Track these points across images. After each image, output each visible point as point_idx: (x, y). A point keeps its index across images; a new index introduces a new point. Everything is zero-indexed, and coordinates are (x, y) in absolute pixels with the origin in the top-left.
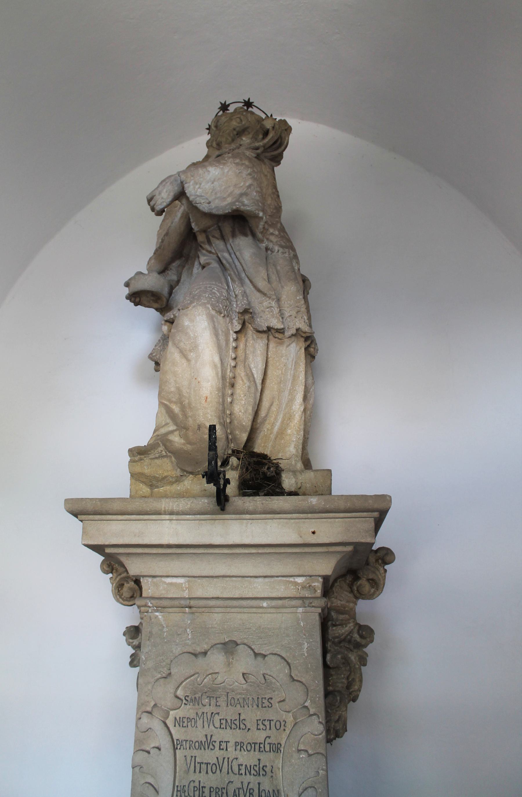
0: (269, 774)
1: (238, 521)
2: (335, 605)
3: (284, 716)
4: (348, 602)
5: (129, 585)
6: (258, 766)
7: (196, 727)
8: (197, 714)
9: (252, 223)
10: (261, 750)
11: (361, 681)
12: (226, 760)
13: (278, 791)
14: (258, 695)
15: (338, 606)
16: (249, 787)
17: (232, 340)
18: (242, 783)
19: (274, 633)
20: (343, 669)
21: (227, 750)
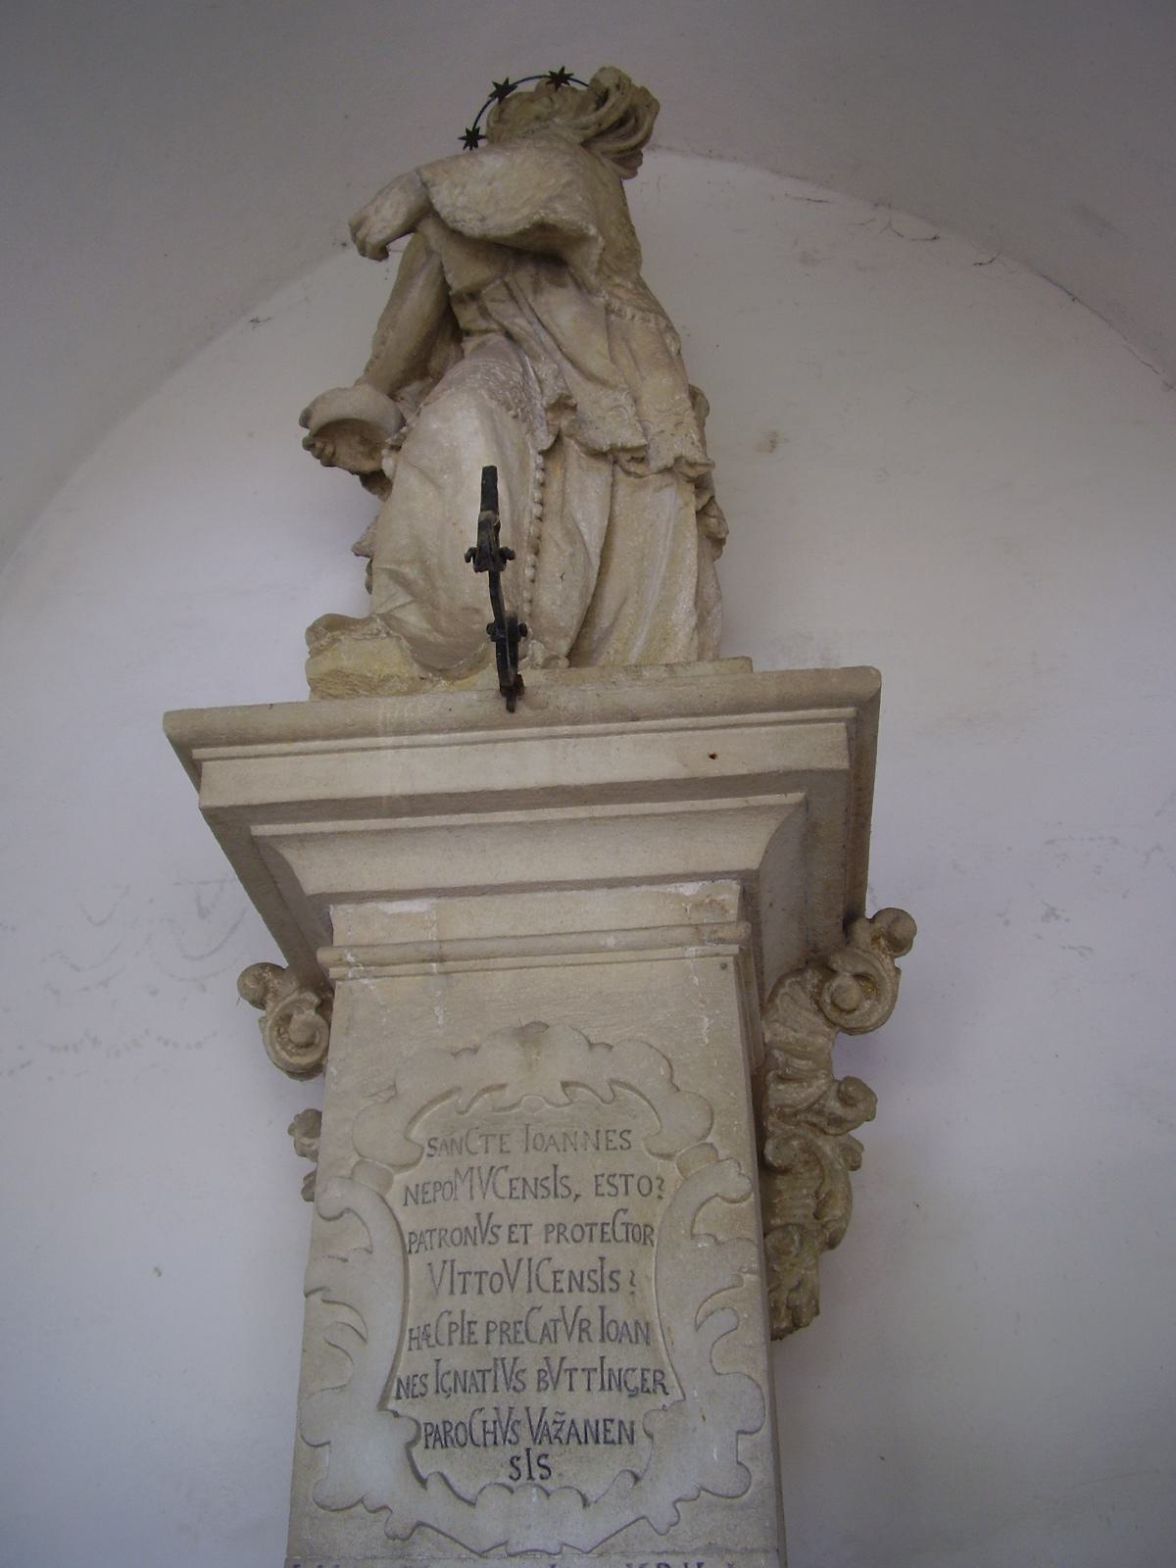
0: (625, 1287)
1: (546, 742)
2: (784, 1038)
3: (659, 1166)
4: (811, 1033)
5: (303, 1017)
6: (599, 1272)
7: (456, 1199)
8: (457, 1172)
9: (575, 257)
10: (606, 1237)
11: (848, 1199)
12: (524, 1263)
13: (647, 1324)
14: (598, 1125)
15: (789, 1043)
16: (579, 1317)
17: (533, 465)
18: (562, 1308)
19: (632, 1001)
20: (807, 1175)
21: (526, 1242)
